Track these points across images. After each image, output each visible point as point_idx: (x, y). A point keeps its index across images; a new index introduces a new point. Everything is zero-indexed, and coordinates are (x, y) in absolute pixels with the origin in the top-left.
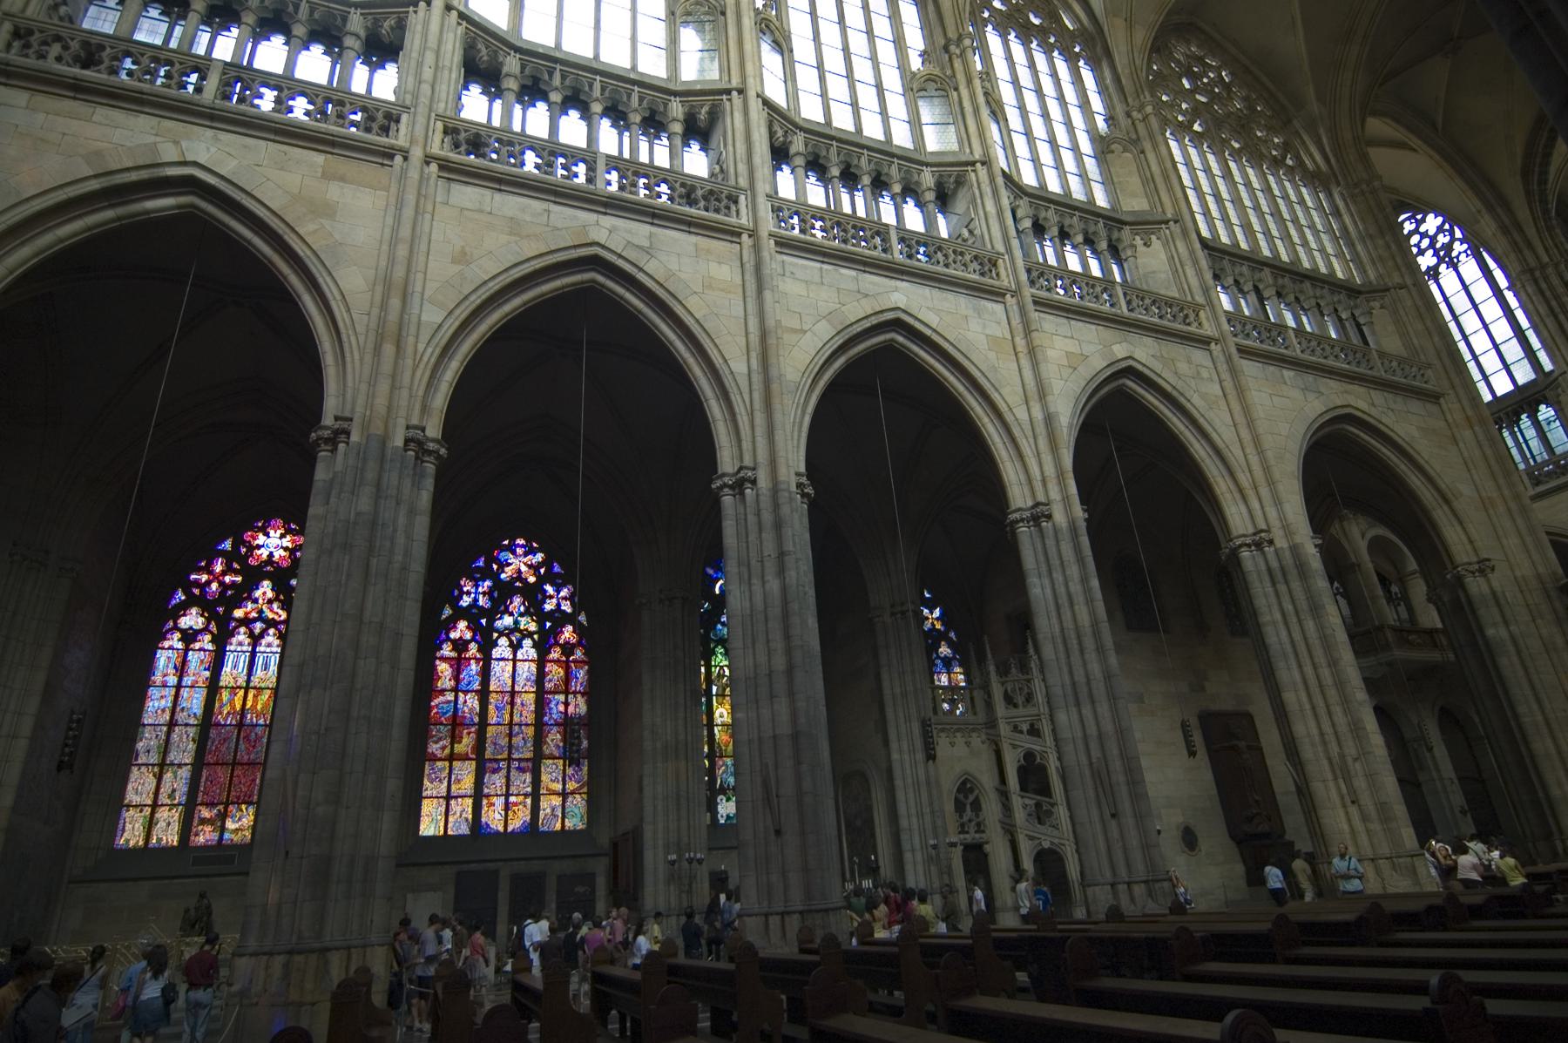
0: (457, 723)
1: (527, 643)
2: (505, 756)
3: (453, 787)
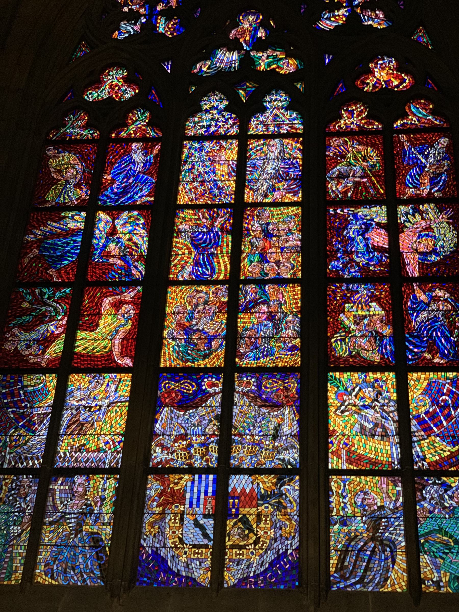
1: (276, 101)
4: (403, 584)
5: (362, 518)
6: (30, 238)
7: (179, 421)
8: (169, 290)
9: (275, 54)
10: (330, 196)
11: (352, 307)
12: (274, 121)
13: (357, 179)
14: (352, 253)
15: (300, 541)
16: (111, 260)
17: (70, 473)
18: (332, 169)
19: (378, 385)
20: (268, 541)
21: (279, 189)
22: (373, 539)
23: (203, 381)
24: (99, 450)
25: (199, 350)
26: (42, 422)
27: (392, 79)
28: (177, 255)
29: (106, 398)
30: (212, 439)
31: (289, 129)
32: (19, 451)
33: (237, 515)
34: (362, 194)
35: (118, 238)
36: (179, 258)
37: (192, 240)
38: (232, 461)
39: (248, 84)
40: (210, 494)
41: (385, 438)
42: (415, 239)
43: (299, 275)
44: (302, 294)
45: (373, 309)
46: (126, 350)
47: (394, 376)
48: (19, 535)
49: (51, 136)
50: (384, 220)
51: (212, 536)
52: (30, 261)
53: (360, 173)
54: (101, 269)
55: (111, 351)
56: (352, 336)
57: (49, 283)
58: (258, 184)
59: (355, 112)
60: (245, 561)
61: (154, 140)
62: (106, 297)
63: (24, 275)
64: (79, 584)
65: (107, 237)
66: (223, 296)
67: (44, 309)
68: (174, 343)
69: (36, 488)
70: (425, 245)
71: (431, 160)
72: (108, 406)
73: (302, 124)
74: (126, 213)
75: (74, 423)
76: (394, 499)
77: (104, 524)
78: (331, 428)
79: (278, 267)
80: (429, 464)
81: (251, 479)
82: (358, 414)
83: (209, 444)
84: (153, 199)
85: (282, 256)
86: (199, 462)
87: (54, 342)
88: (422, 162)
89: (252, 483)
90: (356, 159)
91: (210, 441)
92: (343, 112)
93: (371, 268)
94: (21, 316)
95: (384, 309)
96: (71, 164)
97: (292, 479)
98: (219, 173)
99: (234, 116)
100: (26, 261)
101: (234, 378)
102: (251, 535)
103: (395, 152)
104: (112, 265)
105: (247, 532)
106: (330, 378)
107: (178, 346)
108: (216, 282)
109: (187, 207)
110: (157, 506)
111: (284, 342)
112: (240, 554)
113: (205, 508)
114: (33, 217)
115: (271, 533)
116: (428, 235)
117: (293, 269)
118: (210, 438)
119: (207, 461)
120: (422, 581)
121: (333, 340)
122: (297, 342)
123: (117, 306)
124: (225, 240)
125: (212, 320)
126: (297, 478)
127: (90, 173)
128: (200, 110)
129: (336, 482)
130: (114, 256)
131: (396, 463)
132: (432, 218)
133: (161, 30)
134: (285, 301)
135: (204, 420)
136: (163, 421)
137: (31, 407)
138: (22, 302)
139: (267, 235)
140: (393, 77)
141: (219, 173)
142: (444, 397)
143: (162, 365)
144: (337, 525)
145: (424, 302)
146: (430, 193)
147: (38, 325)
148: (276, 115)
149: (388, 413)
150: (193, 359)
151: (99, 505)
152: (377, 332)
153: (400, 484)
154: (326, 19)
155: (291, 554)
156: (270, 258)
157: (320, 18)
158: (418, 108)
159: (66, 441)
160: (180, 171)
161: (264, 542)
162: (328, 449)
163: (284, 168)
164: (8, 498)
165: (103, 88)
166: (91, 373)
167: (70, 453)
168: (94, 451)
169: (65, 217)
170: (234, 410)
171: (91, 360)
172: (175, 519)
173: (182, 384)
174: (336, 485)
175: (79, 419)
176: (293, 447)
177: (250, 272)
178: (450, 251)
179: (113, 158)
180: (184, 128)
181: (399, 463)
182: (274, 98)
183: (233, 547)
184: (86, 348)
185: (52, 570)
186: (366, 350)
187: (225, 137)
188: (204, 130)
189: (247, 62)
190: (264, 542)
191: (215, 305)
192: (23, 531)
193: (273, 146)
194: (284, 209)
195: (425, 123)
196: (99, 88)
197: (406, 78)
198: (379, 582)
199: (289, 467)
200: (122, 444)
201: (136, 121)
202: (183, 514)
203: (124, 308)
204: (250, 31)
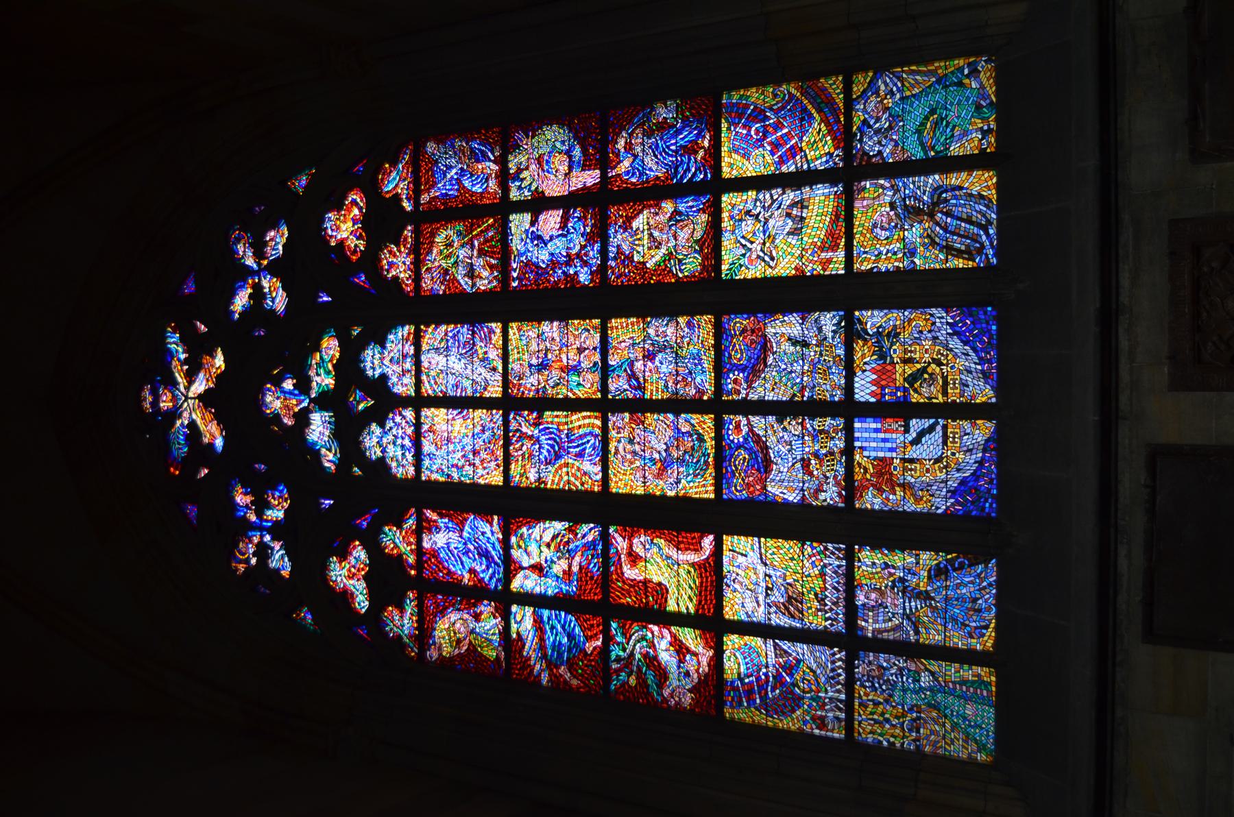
1: (374, 361)
3: (816, 621)
6: (545, 679)
13: (475, 253)
14: (568, 255)
15: (936, 307)
16: (575, 569)
21: (486, 353)
22: (931, 215)
23: (732, 441)
24: (822, 575)
26: (786, 652)
28: (569, 482)
33: (905, 390)
36: (572, 479)
38: (836, 399)
40: (879, 426)
42: (552, 177)
43: (596, 322)
48: (932, 674)
50: (527, 217)
51: (932, 421)
52: (575, 677)
55: (693, 565)
57: (605, 651)
58: (479, 380)
61: (421, 518)
62: (623, 574)
65: (545, 576)
67: (638, 656)
70: (560, 164)
72: (766, 564)
73: (403, 326)
74: (513, 552)
75: (787, 609)
77: (918, 563)
84: (496, 517)
89: (864, 371)
90: (449, 256)
94: (648, 686)
95: (641, 211)
97: (859, 320)
98: (463, 430)
99: (391, 416)
100: (575, 682)
102: (929, 370)
104: (581, 568)
105: (926, 376)
107: (689, 475)
108: (605, 429)
111: (683, 337)
115: (927, 344)
116: (548, 162)
120: (983, 151)
122: (682, 320)
123: (634, 559)
126: (857, 313)
130: (570, 566)
133: (281, 515)
138: (630, 686)
139: (543, 366)
141: (463, 430)
143: (712, 496)
146: (494, 162)
147: (659, 663)
148: (391, 361)
149: (773, 201)
150: (704, 455)
152: (670, 219)
155: (952, 317)
157: (273, 311)
160: (461, 483)
161: (939, 353)
162: (819, 275)
166: (722, 590)
168: (824, 581)
169: (518, 633)
172: (911, 470)
182: (369, 365)
183: (945, 393)
184: (690, 597)
185: (976, 628)
187: (418, 425)
189: (324, 401)
190: (939, 353)
192: (927, 669)
196: (352, 594)
198: (985, 206)
200: (815, 544)
202: (904, 460)
203: (638, 549)
204: (285, 399)
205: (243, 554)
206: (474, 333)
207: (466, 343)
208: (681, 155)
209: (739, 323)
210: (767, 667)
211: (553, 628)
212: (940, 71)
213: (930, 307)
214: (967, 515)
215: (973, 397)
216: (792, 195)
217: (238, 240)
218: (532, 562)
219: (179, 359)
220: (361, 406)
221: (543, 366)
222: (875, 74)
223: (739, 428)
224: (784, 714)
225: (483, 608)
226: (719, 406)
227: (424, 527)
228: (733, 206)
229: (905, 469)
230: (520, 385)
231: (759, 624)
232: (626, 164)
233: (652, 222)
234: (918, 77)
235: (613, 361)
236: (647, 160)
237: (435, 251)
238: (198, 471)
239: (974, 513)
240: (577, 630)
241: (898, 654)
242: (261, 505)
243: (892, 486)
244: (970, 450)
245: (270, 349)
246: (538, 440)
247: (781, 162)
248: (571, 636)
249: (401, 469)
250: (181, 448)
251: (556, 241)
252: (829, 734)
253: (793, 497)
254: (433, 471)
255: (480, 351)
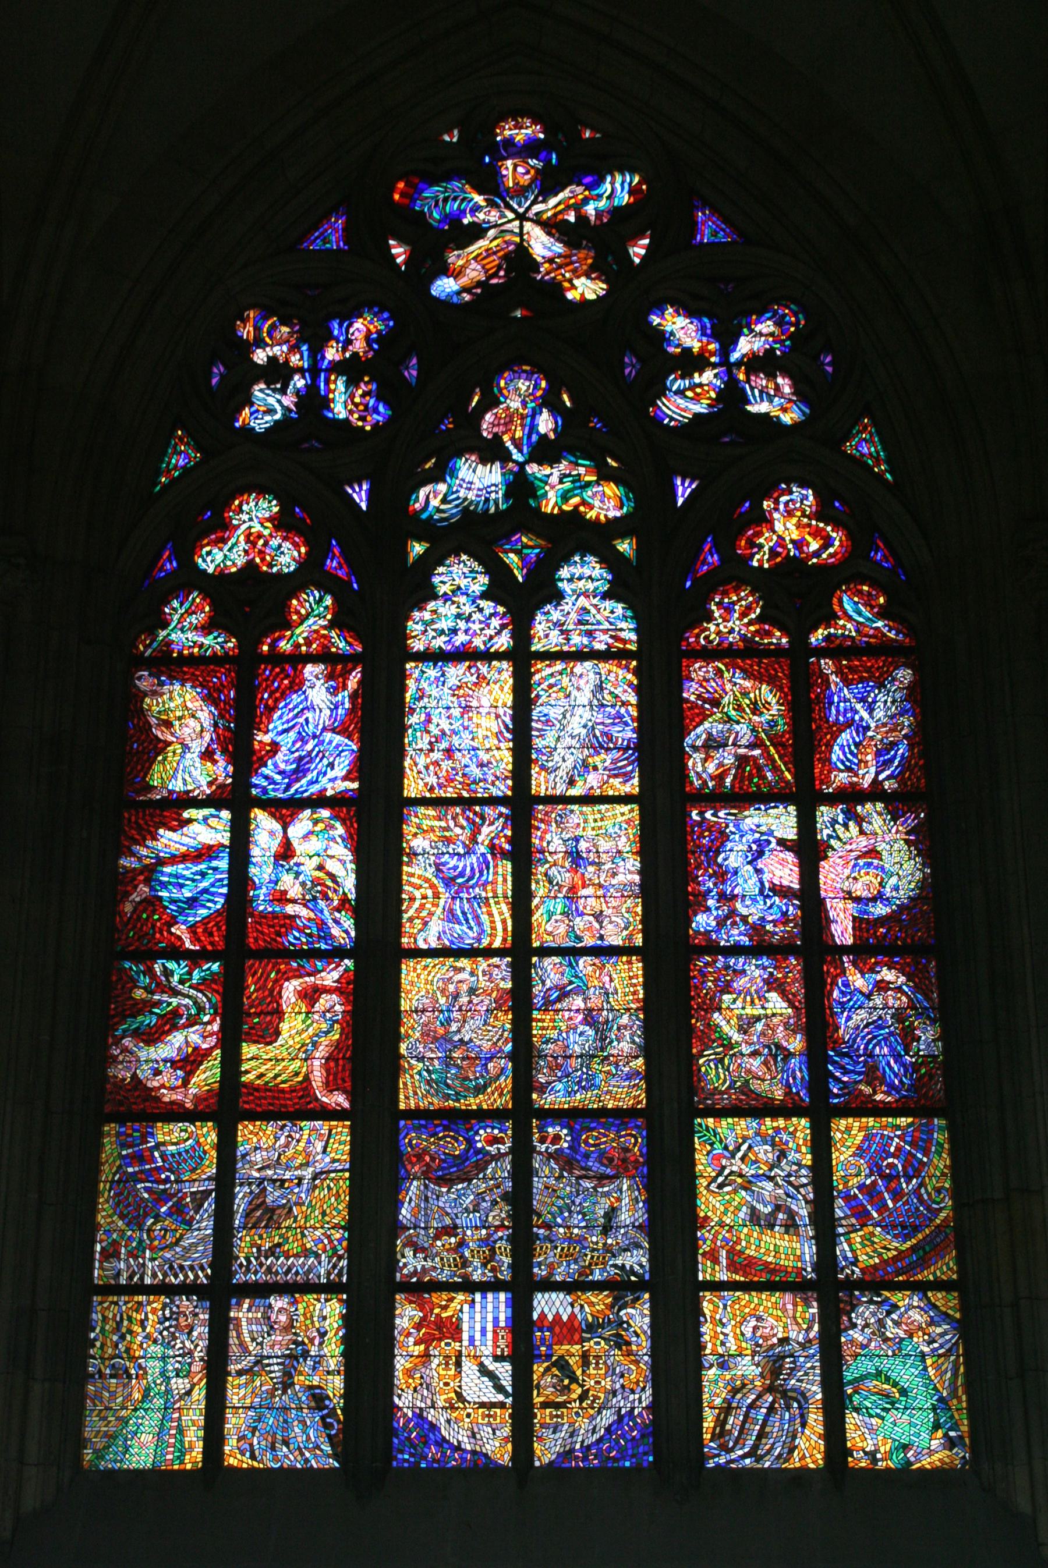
0: (246, 946)
1: (583, 576)
2: (498, 1098)
3: (244, 1244)
4: (819, 1456)
5: (753, 1357)
6: (127, 862)
7: (441, 1204)
8: (404, 966)
9: (574, 473)
10: (692, 783)
11: (735, 1001)
12: (580, 622)
13: (742, 751)
14: (735, 897)
15: (653, 1395)
16: (290, 909)
17: (261, 1291)
18: (695, 728)
19: (781, 1139)
20: (602, 1396)
21: (595, 768)
22: (770, 1389)
23: (477, 1133)
24: (306, 1253)
25: (467, 1078)
27: (807, 537)
28: (412, 899)
29: (308, 1164)
30: (500, 1234)
31: (611, 641)
32: (168, 1255)
33: (548, 1357)
34: (751, 781)
35: (298, 865)
36: (417, 904)
37: (438, 870)
39: (524, 540)
40: (502, 1324)
41: (792, 1230)
42: (847, 872)
43: (639, 940)
44: (644, 976)
45: (770, 1005)
46: (335, 1079)
47: (808, 1125)
48: (189, 1393)
49: (141, 647)
50: (791, 834)
51: (509, 1389)
53: (747, 737)
54: (273, 926)
55: (307, 1079)
56: (734, 1055)
58: (556, 758)
59: (737, 607)
60: (566, 1427)
62: (287, 980)
63: (128, 937)
64: (299, 1466)
66: (503, 979)
67: (175, 1001)
68: (421, 1065)
69: (207, 1317)
71: (879, 714)
73: (636, 630)
74: (307, 812)
76: (805, 1326)
77: (328, 1373)
78: (702, 1214)
79: (601, 923)
80: (862, 1270)
81: (569, 1299)
82: (746, 1189)
83: (495, 1242)
84: (355, 785)
85: (607, 902)
86: (479, 1271)
87: (201, 1063)
88: (862, 719)
89: (572, 1306)
90: (739, 708)
91: (496, 1237)
92: (714, 608)
93: (768, 928)
95: (791, 1004)
96: (188, 709)
97: (638, 1299)
99: (501, 609)
100: (128, 908)
101: (531, 1127)
102: (574, 1386)
103: (813, 696)
104: (293, 918)
105: (566, 1382)
106: (697, 1128)
107: (428, 1071)
108: (488, 953)
109: (423, 802)
110: (416, 1344)
112: (557, 1416)
113: (496, 1346)
114: (129, 820)
115: (607, 1383)
116: (869, 865)
117: (626, 928)
118: (495, 1232)
119: (493, 1270)
121: (701, 1061)
123: (310, 995)
124: (500, 870)
125: (485, 1023)
126: (647, 1296)
127: (227, 729)
128: (435, 597)
129: (710, 1301)
130: (294, 901)
131: (809, 1269)
132: (879, 831)
134: (616, 990)
135: (484, 1200)
136: (413, 1204)
137: (178, 1181)
139: (576, 858)
140: (809, 534)
141: (481, 733)
142: (890, 1160)
143: (402, 1106)
144: (713, 1370)
145: (861, 992)
146: (875, 780)
147: (169, 1032)
148: (585, 610)
149: (797, 1188)
150: (457, 1094)
151: (317, 1342)
152: (778, 1046)
153: (815, 1304)
154: (676, 393)
155: (640, 1414)
156: (585, 907)
157: (662, 391)
158: (856, 603)
159: (248, 1239)
160: (403, 728)
161: (596, 1398)
162: (697, 1248)
163: (603, 723)
164: (161, 1333)
165: (233, 540)
167: (257, 1259)
168: (297, 1256)
169: (190, 821)
170: (535, 1184)
171: (275, 1098)
172: (447, 1364)
173: (440, 1139)
174: (711, 1307)
175: (264, 1202)
176: (638, 1246)
177: (549, 934)
178: (909, 897)
179: (270, 696)
180: (404, 636)
181: (813, 1271)
182: (577, 571)
183: (545, 1405)
184: (261, 1076)
185: (251, 1445)
186: (759, 1078)
187: (488, 656)
188: (444, 638)
189: (521, 488)
190: (596, 1398)
191: (490, 995)
193: (581, 676)
194: (607, 810)
195: (870, 637)
196: (225, 541)
197: (834, 535)
199: (633, 1278)
200: (345, 1243)
201: (307, 616)
203: (325, 1001)
204: (523, 417)
205: (270, 335)
206: (628, 748)
207: (609, 737)
208: (865, 1062)
209: (634, 1142)
210: (177, 1181)
211: (203, 875)
212: (955, 1402)
213: (653, 1387)
214: (394, 1432)
215: (540, 1439)
216: (804, 1212)
217: (780, 323)
218: (295, 843)
219: (586, 201)
220: (512, 559)
221: (576, 858)
222: (958, 1321)
223: (493, 1140)
224: (118, 1204)
225: (222, 764)
226: (523, 1114)
227: (336, 666)
228: (793, 1134)
229: (447, 1357)
230: (548, 823)
231: (234, 1171)
232: (858, 981)
233: (775, 1020)
234: (949, 1375)
235: (585, 964)
236: (863, 1014)
237: (747, 684)
238: (402, 240)
239: (396, 1441)
240: (204, 912)
241: (210, 1350)
242: (351, 370)
243: (426, 1341)
244: (474, 1435)
245: (605, 385)
246: (469, 851)
247: (848, 1198)
248: (193, 902)
249: (420, 627)
250: (437, 202)
251: (755, 878)
252: (97, 1264)
253: (405, 1213)
254: (420, 678)
255: (597, 760)
